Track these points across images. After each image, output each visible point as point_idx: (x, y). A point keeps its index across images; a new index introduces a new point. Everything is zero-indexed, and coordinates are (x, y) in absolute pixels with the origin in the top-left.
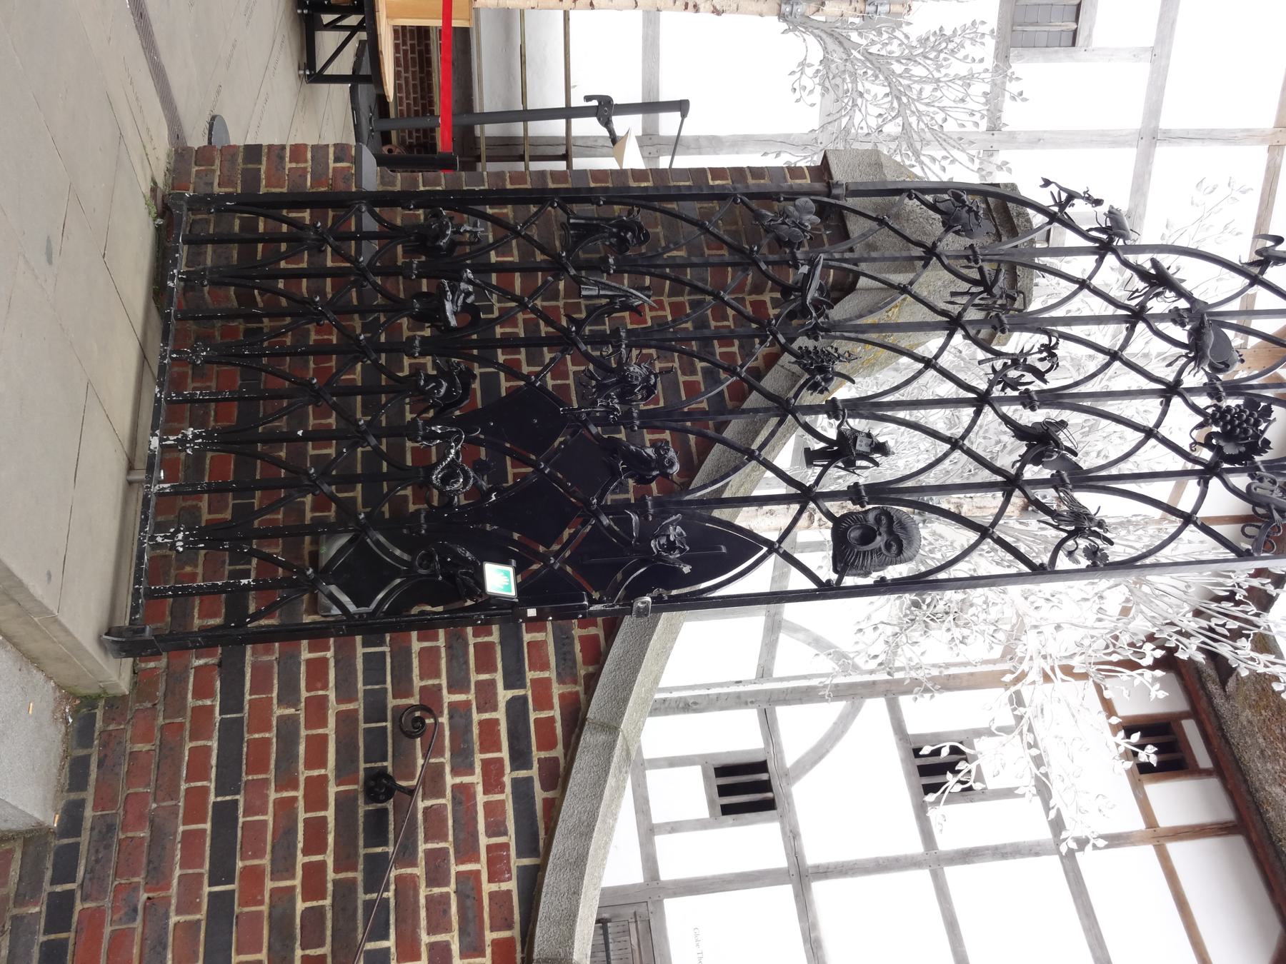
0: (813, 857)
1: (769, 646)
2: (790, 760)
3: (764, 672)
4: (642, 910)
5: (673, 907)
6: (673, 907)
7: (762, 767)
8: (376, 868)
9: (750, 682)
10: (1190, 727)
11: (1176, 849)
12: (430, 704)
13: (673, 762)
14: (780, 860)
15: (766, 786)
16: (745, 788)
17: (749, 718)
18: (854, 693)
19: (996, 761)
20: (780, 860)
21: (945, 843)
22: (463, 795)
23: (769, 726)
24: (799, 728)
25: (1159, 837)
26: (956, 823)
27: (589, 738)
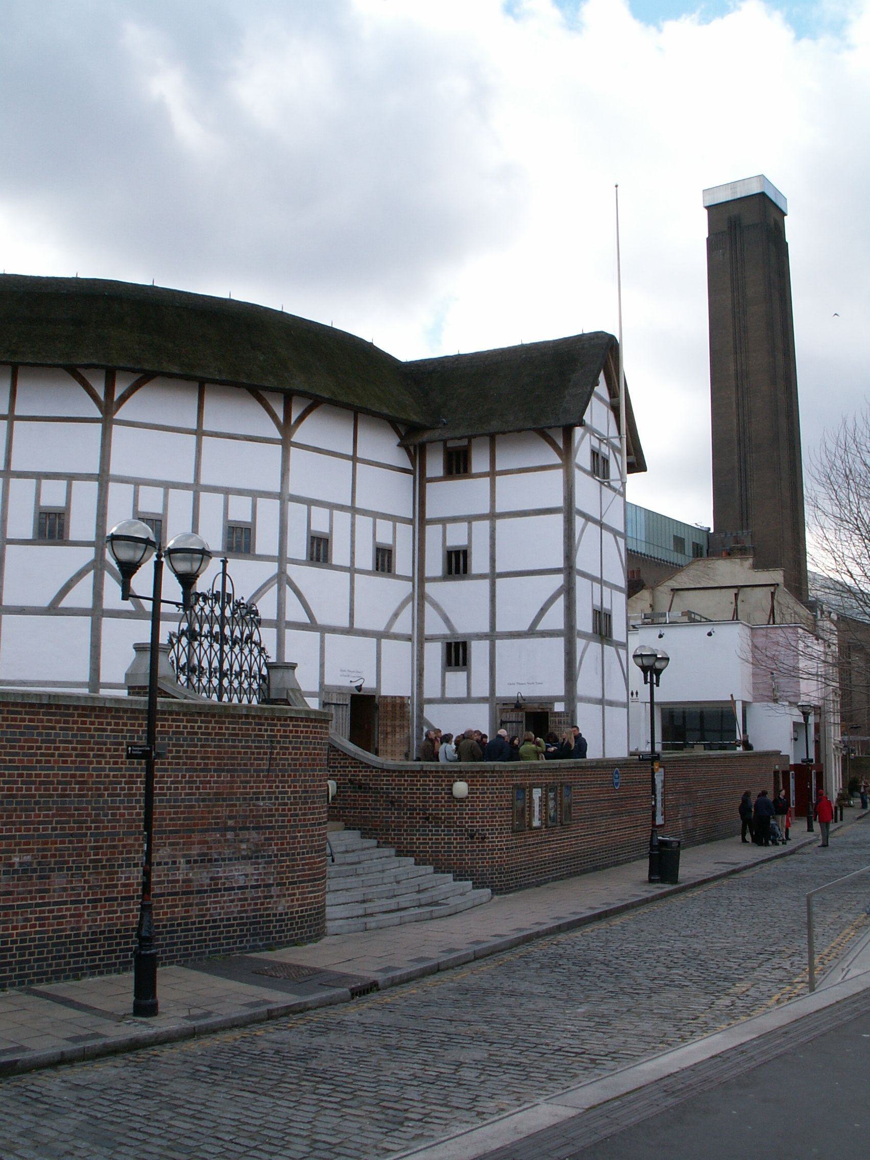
0: (486, 629)
1: (396, 637)
2: (446, 631)
3: (409, 639)
4: (498, 707)
5: (498, 694)
6: (498, 694)
7: (449, 645)
8: (370, 788)
9: (413, 645)
10: (450, 444)
11: (498, 468)
12: (350, 780)
13: (443, 685)
14: (486, 644)
15: (457, 644)
16: (457, 654)
17: (428, 646)
18: (422, 596)
19: (457, 537)
20: (486, 644)
21: (486, 570)
22: (363, 776)
23: (432, 639)
24: (434, 625)
25: (492, 474)
26: (479, 563)
27: (356, 757)
